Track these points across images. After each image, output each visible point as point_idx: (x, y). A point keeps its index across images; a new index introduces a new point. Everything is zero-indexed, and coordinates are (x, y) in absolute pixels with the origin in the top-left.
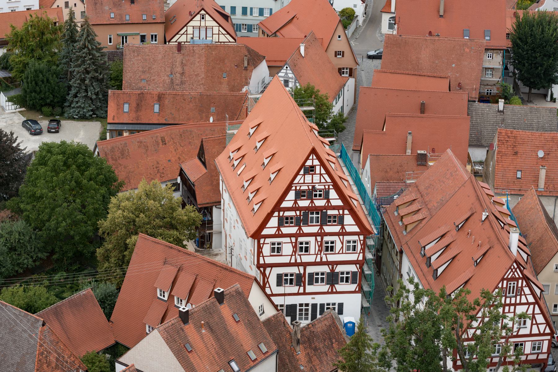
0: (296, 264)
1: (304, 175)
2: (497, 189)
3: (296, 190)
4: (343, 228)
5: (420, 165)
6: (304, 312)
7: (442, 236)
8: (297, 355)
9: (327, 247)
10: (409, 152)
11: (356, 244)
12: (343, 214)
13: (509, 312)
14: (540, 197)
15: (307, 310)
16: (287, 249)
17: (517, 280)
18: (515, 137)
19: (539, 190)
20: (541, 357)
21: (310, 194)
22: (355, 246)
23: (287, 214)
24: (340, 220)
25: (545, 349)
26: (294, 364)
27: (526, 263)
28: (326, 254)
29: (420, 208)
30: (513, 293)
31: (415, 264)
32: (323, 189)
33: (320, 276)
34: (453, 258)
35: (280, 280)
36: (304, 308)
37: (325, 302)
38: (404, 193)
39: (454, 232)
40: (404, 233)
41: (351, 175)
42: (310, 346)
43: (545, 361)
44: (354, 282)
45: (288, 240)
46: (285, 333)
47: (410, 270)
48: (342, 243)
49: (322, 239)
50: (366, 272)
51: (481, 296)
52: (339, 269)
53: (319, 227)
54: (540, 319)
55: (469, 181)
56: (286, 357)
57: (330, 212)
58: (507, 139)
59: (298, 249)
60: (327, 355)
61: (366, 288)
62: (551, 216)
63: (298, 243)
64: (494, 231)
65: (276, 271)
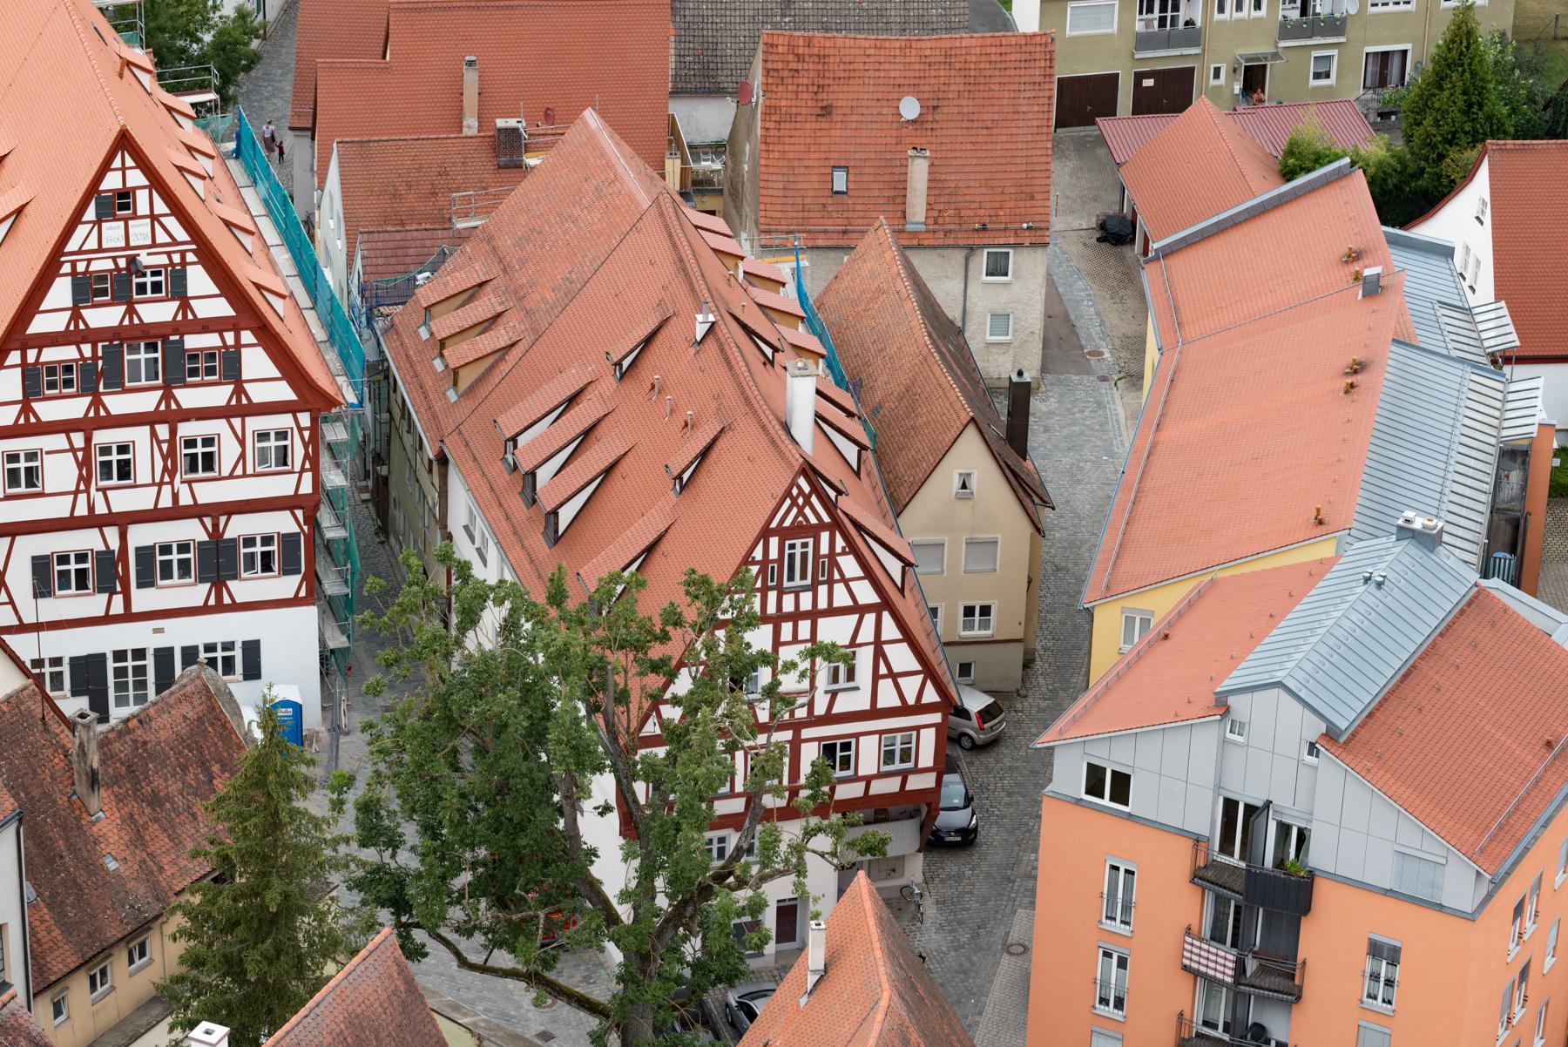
0: (93, 521)
1: (98, 222)
2: (769, 232)
3: (74, 273)
4: (239, 390)
5: (506, 167)
6: (130, 679)
7: (572, 401)
8: (94, 823)
9: (106, 466)
10: (471, 125)
11: (288, 442)
12: (238, 345)
13: (795, 640)
14: (908, 253)
15: (140, 671)
16: (60, 471)
17: (814, 531)
18: (822, 58)
19: (909, 227)
20: (914, 783)
21: (123, 284)
22: (211, 454)
23: (51, 354)
24: (228, 366)
25: (927, 758)
26: (85, 854)
27: (857, 474)
28: (189, 482)
29: (499, 309)
30: (803, 577)
31: (489, 499)
32: (165, 266)
33: (175, 557)
34: (608, 471)
35: (45, 576)
36: (130, 664)
37: (199, 640)
38: (449, 265)
39: (609, 383)
40: (452, 395)
41: (270, 213)
42: (136, 790)
43: (930, 799)
44: (289, 568)
45: (59, 441)
46: (48, 752)
47: (472, 517)
48: (242, 442)
49: (173, 432)
50: (329, 535)
51: (688, 593)
52: (237, 527)
53: (160, 393)
54: (900, 656)
55: (654, 212)
56: (55, 833)
57: (193, 342)
58: (794, 66)
59: (96, 470)
60: (194, 816)
61: (332, 586)
62: (953, 312)
63: (95, 452)
64: (735, 376)
65: (30, 546)
